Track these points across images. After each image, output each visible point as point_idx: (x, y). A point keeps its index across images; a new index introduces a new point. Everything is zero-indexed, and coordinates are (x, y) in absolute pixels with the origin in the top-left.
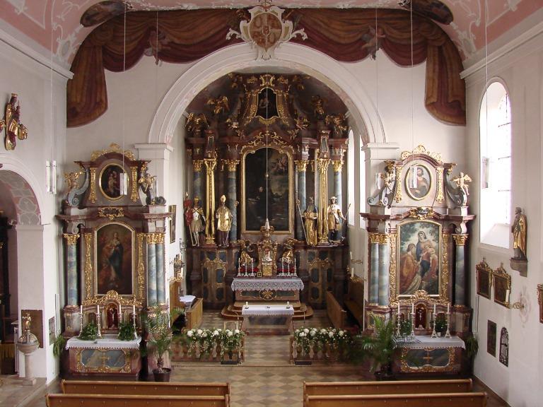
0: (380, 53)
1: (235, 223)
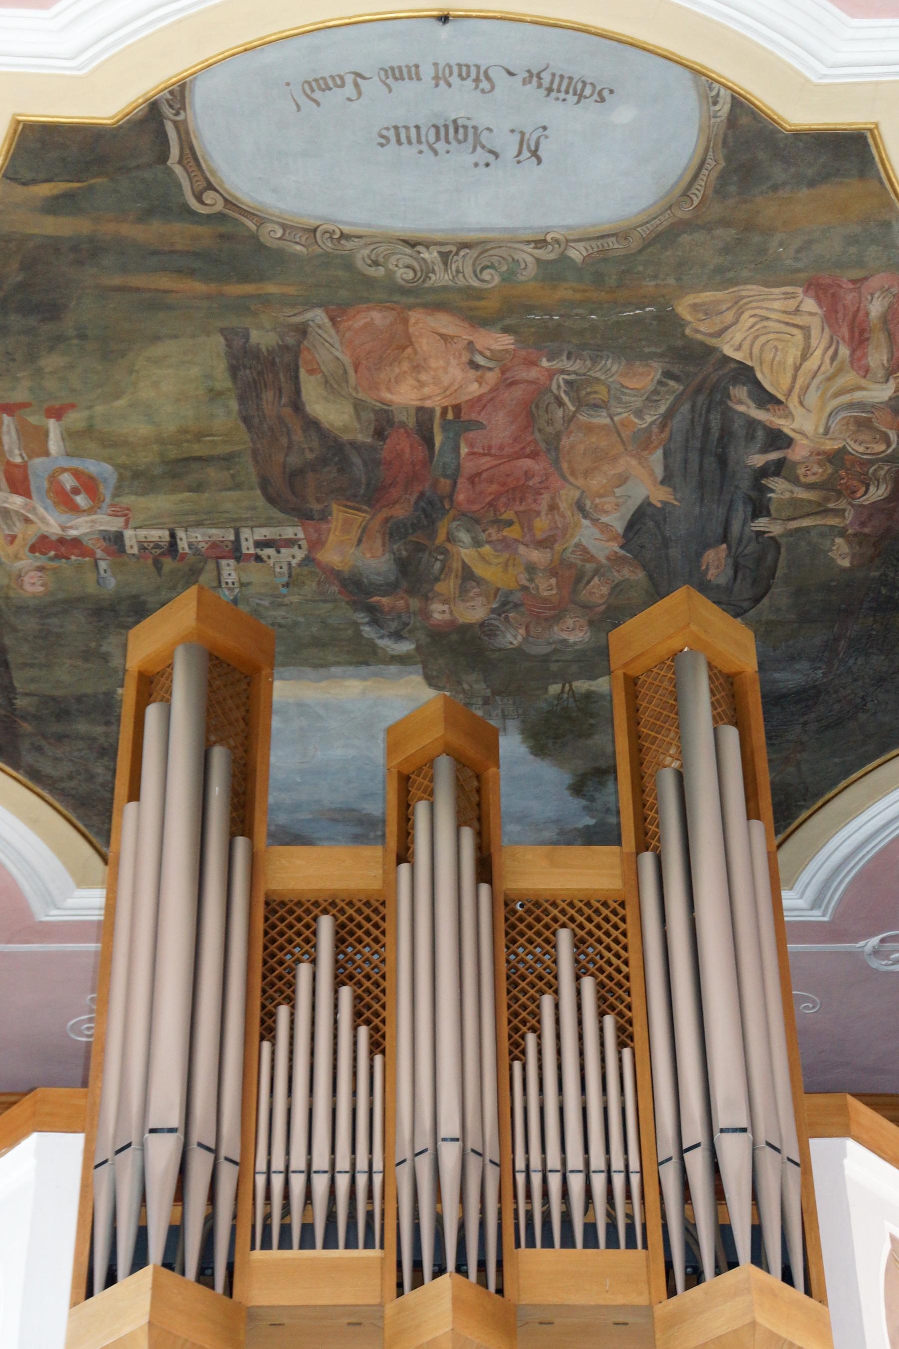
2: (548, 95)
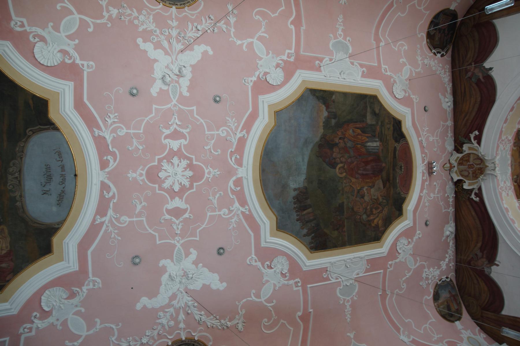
0: (487, 65)
2: (59, 195)
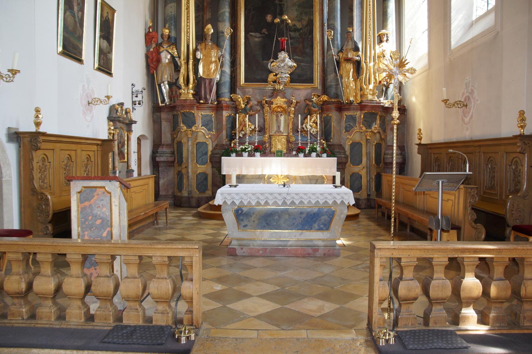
1: (227, 69)
